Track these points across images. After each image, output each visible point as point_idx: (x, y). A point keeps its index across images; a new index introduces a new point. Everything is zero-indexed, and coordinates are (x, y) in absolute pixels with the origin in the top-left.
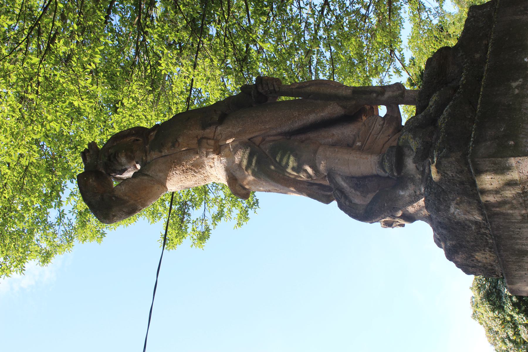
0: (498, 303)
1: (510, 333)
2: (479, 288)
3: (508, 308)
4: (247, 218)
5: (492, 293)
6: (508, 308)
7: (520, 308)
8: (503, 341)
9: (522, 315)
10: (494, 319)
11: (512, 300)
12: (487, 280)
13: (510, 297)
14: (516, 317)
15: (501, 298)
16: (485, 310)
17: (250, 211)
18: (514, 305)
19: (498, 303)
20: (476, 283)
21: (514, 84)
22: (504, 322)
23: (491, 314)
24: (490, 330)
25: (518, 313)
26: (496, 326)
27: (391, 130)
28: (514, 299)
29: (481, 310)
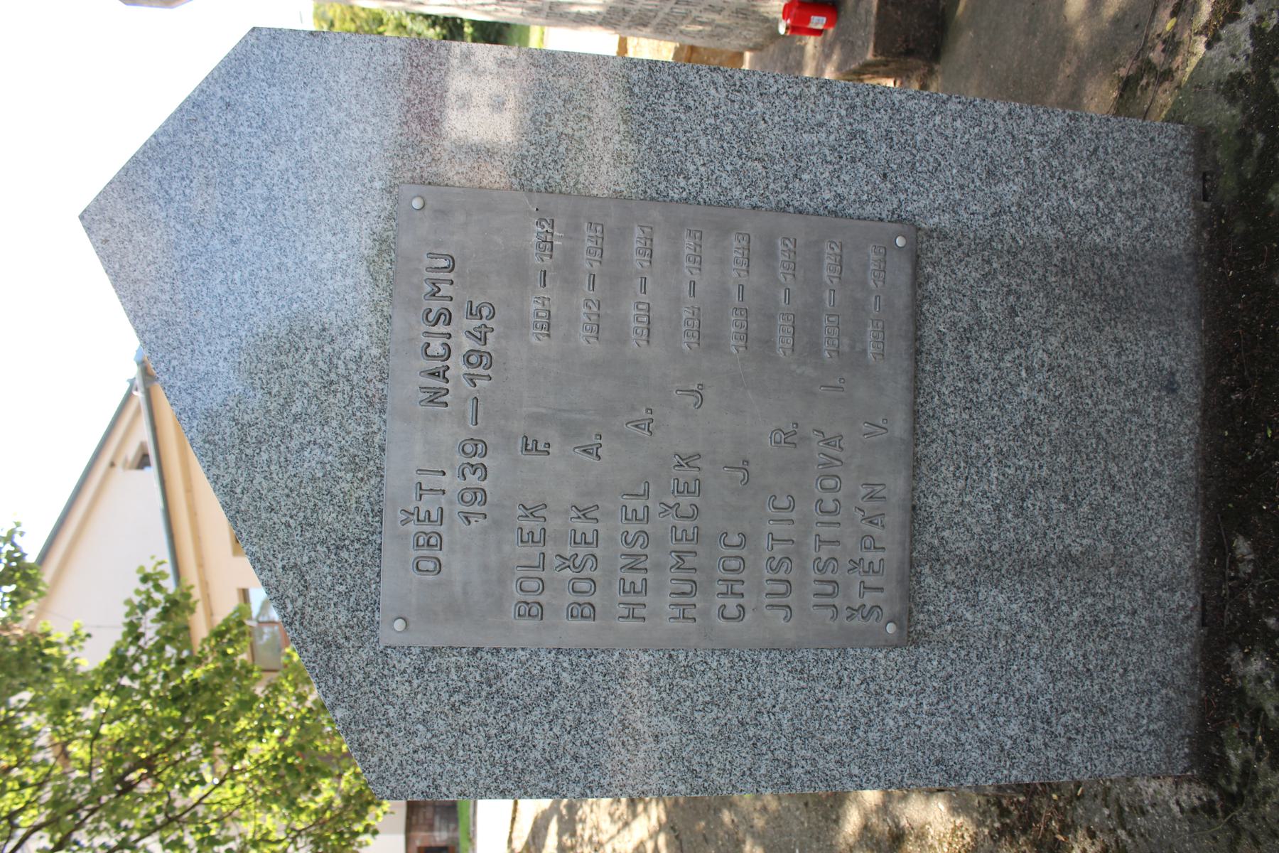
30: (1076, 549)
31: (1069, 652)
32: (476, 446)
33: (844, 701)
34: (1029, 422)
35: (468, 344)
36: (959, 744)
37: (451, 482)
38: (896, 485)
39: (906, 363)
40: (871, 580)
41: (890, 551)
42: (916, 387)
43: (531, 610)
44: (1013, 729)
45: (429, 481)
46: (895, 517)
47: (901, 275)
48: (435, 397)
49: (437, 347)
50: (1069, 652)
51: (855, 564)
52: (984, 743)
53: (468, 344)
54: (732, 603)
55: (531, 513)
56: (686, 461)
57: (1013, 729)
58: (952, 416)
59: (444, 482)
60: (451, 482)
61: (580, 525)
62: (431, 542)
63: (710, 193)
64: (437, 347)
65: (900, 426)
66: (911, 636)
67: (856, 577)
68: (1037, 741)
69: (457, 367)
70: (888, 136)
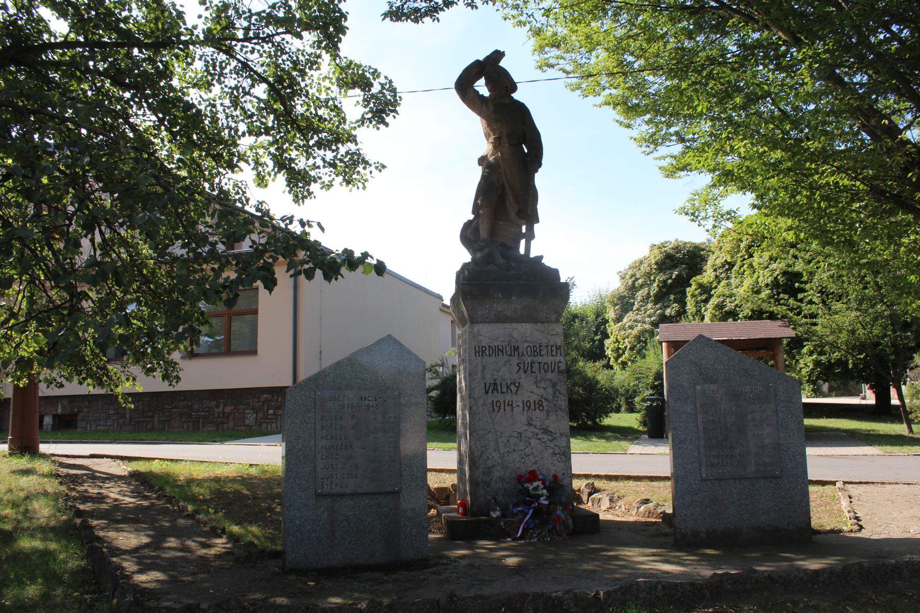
0: (664, 267)
1: (640, 281)
2: (677, 248)
3: (661, 277)
4: (573, 90)
5: (673, 261)
6: (661, 277)
7: (663, 287)
8: (632, 276)
9: (657, 289)
10: (650, 265)
11: (668, 279)
12: (684, 255)
13: (671, 278)
14: (655, 285)
15: (670, 269)
16: (657, 256)
17: (578, 92)
18: (665, 282)
19: (664, 267)
20: (681, 244)
21: (500, 295)
22: (648, 275)
23: (653, 262)
24: (641, 262)
25: (658, 286)
26: (644, 268)
28: (669, 281)
29: (656, 251)
31: (314, 534)
36: (294, 510)
38: (348, 490)
40: (329, 487)
41: (336, 490)
42: (368, 494)
47: (390, 489)
49: (370, 398)
50: (314, 534)
54: (324, 457)
55: (341, 417)
56: (351, 446)
57: (297, 522)
59: (346, 401)
60: (346, 402)
61: (338, 427)
62: (335, 399)
64: (370, 398)
65: (360, 490)
66: (319, 496)
69: (367, 402)
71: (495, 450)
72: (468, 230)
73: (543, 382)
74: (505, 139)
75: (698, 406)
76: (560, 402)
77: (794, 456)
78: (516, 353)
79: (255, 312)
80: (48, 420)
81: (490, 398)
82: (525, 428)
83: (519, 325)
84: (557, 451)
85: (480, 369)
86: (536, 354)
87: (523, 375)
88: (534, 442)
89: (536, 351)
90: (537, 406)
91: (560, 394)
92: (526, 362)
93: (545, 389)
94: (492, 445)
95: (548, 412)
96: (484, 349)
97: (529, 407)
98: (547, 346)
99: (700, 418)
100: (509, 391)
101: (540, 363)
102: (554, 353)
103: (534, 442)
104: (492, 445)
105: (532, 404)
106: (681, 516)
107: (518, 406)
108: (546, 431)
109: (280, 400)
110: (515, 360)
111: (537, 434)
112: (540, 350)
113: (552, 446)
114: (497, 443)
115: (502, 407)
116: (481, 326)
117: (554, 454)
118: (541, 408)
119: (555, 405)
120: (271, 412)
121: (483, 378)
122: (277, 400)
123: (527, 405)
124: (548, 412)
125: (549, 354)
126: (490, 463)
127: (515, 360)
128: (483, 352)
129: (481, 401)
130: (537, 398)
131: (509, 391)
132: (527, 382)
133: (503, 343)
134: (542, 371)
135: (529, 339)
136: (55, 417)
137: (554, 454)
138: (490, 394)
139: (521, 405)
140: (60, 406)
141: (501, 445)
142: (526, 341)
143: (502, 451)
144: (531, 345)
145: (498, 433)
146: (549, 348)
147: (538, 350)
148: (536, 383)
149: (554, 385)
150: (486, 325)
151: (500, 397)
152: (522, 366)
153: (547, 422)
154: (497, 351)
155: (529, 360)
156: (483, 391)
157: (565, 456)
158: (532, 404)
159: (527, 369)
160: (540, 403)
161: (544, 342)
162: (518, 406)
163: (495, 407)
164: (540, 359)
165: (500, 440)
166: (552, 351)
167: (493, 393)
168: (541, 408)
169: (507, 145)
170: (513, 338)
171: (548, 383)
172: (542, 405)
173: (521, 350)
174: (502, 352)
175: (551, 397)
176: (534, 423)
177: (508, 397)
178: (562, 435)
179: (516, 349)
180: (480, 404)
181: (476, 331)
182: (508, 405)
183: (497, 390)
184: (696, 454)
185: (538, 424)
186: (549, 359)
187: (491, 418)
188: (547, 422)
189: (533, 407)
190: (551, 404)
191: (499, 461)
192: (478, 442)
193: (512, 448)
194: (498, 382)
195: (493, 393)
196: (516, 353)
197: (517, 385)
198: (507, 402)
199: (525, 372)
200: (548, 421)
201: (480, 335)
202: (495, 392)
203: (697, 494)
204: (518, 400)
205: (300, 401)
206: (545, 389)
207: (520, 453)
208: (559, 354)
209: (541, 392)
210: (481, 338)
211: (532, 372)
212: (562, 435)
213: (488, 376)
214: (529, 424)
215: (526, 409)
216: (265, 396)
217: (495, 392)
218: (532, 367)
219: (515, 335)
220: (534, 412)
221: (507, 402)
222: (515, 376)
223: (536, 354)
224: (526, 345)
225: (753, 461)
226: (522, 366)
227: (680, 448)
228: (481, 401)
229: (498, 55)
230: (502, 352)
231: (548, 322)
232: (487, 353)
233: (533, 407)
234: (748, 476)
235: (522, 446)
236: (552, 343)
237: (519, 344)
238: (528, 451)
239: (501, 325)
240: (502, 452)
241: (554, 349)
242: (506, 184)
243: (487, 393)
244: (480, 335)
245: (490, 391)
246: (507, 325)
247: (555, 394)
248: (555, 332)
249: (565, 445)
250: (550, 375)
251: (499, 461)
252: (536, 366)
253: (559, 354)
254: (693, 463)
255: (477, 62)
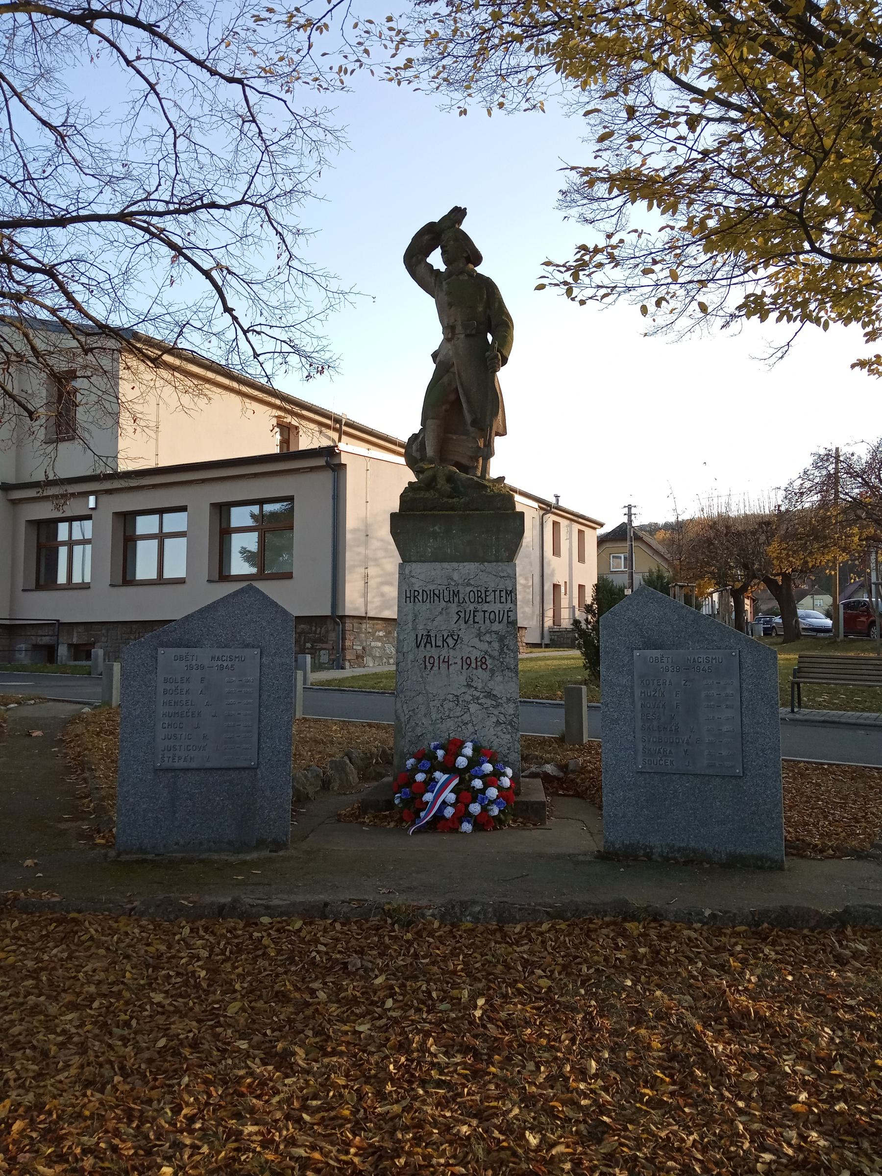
27: (469, 454)
30: (177, 815)
32: (202, 667)
33: (141, 754)
34: (209, 800)
35: (225, 665)
37: (194, 663)
38: (194, 765)
39: (223, 766)
43: (166, 681)
44: (131, 800)
45: (195, 658)
46: (185, 765)
48: (213, 658)
49: (224, 658)
51: (174, 755)
52: (128, 792)
53: (225, 665)
54: (166, 725)
57: (131, 800)
58: (211, 779)
60: (194, 663)
63: (262, 717)
64: (224, 658)
65: (208, 765)
66: (157, 770)
67: (171, 755)
68: (128, 807)
69: (220, 663)
70: (279, 761)
71: (425, 715)
72: (414, 447)
73: (488, 635)
74: (459, 329)
75: (636, 677)
76: (507, 660)
77: (763, 751)
78: (456, 600)
79: (291, 528)
80: (63, 651)
81: (422, 652)
82: (464, 690)
83: (461, 564)
84: (502, 718)
85: (410, 617)
86: (480, 600)
87: (463, 626)
88: (473, 708)
89: (481, 597)
90: (479, 664)
91: (509, 649)
92: (468, 610)
93: (490, 643)
94: (423, 710)
95: (492, 672)
96: (416, 593)
97: (470, 665)
98: (494, 591)
99: (637, 692)
100: (445, 644)
101: (485, 612)
102: (503, 600)
103: (473, 708)
104: (423, 710)
105: (473, 661)
106: (609, 815)
107: (456, 663)
108: (490, 695)
109: (318, 631)
110: (454, 608)
111: (478, 698)
112: (486, 596)
113: (496, 712)
114: (429, 707)
115: (436, 664)
116: (414, 565)
117: (498, 723)
118: (484, 666)
119: (502, 663)
120: (308, 645)
121: (415, 629)
122: (316, 630)
123: (467, 662)
124: (492, 672)
125: (497, 600)
126: (419, 731)
127: (454, 608)
128: (415, 597)
129: (411, 657)
130: (478, 654)
131: (445, 644)
132: (468, 635)
133: (439, 587)
134: (487, 621)
135: (472, 582)
136: (70, 646)
137: (498, 723)
138: (422, 647)
139: (460, 662)
140: (75, 634)
141: (434, 710)
142: (469, 585)
143: (434, 717)
144: (475, 590)
145: (430, 695)
146: (497, 593)
147: (483, 596)
148: (479, 635)
149: (501, 639)
150: (419, 565)
151: (434, 652)
152: (462, 615)
153: (491, 684)
154: (434, 596)
155: (472, 607)
156: (414, 644)
157: (512, 726)
158: (473, 661)
159: (469, 619)
160: (484, 660)
161: (492, 586)
162: (456, 663)
163: (427, 664)
164: (485, 607)
165: (432, 704)
166: (501, 597)
167: (425, 646)
168: (484, 666)
169: (463, 336)
170: (452, 579)
171: (494, 636)
172: (485, 663)
173: (461, 596)
174: (439, 597)
175: (496, 654)
176: (474, 684)
177: (444, 652)
178: (509, 700)
179: (456, 594)
180: (409, 660)
181: (407, 572)
182: (444, 661)
183: (431, 643)
184: (630, 738)
185: (480, 686)
186: (497, 607)
187: (422, 677)
188: (491, 684)
189: (473, 665)
190: (496, 662)
191: (430, 729)
192: (405, 706)
193: (447, 714)
194: (432, 634)
195: (425, 646)
196: (456, 600)
197: (456, 637)
198: (442, 658)
199: (466, 623)
200: (492, 682)
201: (413, 577)
202: (428, 645)
203: (631, 790)
204: (456, 656)
205: (140, 661)
206: (490, 643)
207: (456, 720)
208: (509, 601)
209: (485, 646)
210: (413, 580)
211: (474, 622)
212: (509, 700)
213: (420, 627)
214: (469, 686)
215: (465, 667)
216: (302, 626)
217: (428, 645)
218: (474, 616)
219: (456, 576)
220: (475, 671)
221: (442, 658)
222: (453, 626)
223: (480, 600)
224: (469, 589)
225: (706, 753)
226: (462, 615)
227: (611, 730)
228: (411, 657)
229: (458, 214)
230: (439, 597)
231: (497, 561)
232: (420, 598)
233: (473, 665)
234: (699, 772)
235: (458, 711)
236: (501, 587)
237: (460, 588)
238: (466, 717)
239: (437, 565)
240: (434, 719)
241: (503, 594)
242: (460, 390)
243: (418, 647)
244: (413, 577)
245: (422, 644)
246: (445, 565)
247: (502, 649)
248: (505, 574)
249: (513, 712)
250: (496, 627)
251: (430, 729)
252: (480, 615)
253: (509, 601)
254: (627, 749)
255: (431, 225)
